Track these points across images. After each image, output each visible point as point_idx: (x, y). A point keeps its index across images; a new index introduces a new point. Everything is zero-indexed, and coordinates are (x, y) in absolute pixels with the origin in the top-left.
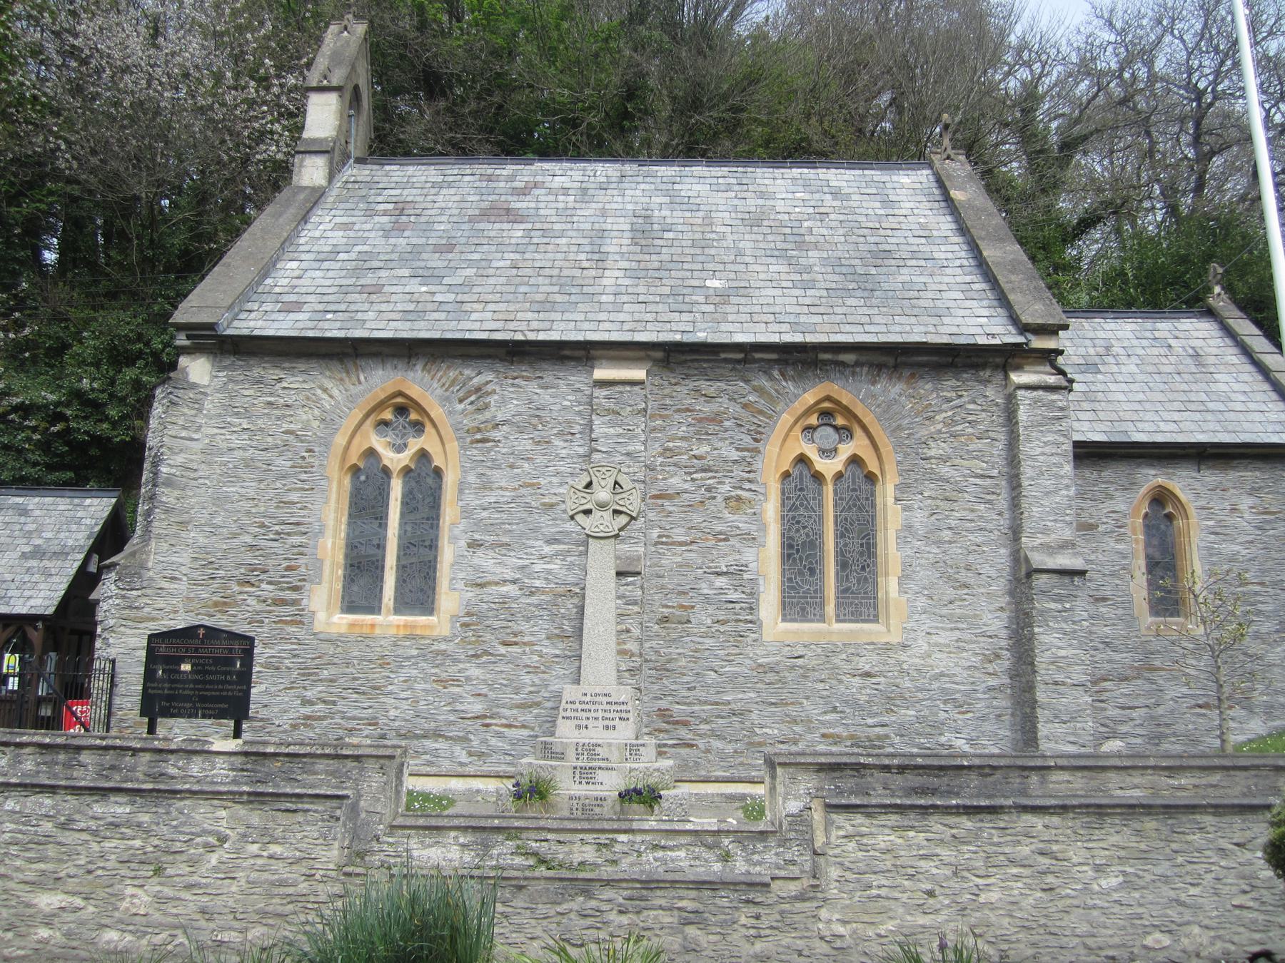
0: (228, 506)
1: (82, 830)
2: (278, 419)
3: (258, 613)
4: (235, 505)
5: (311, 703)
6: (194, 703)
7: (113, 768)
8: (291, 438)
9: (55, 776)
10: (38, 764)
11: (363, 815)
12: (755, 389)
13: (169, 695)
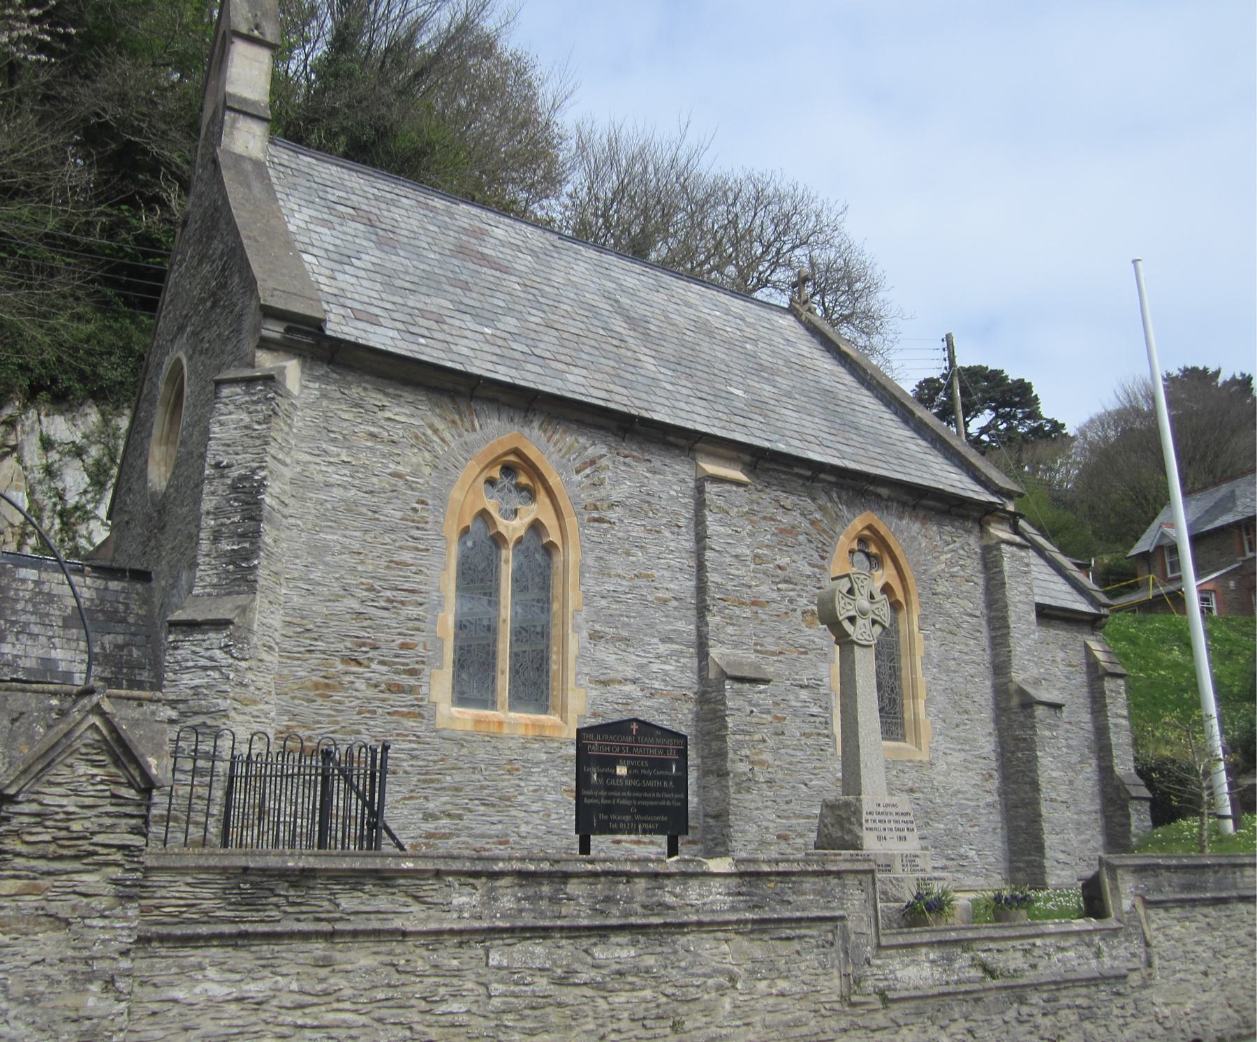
0: (328, 559)
1: (585, 984)
2: (384, 456)
3: (369, 700)
4: (337, 558)
5: (434, 817)
6: (632, 815)
7: (607, 899)
8: (401, 482)
9: (542, 914)
10: (519, 900)
11: (853, 937)
12: (820, 508)
13: (607, 805)
